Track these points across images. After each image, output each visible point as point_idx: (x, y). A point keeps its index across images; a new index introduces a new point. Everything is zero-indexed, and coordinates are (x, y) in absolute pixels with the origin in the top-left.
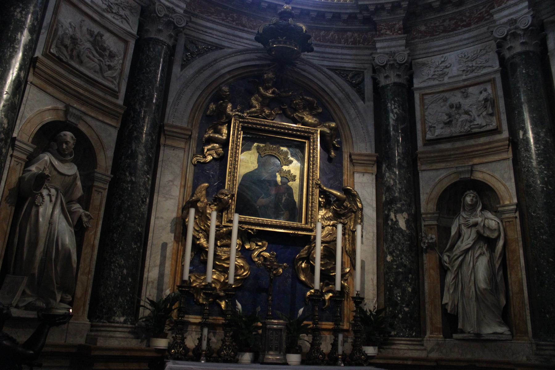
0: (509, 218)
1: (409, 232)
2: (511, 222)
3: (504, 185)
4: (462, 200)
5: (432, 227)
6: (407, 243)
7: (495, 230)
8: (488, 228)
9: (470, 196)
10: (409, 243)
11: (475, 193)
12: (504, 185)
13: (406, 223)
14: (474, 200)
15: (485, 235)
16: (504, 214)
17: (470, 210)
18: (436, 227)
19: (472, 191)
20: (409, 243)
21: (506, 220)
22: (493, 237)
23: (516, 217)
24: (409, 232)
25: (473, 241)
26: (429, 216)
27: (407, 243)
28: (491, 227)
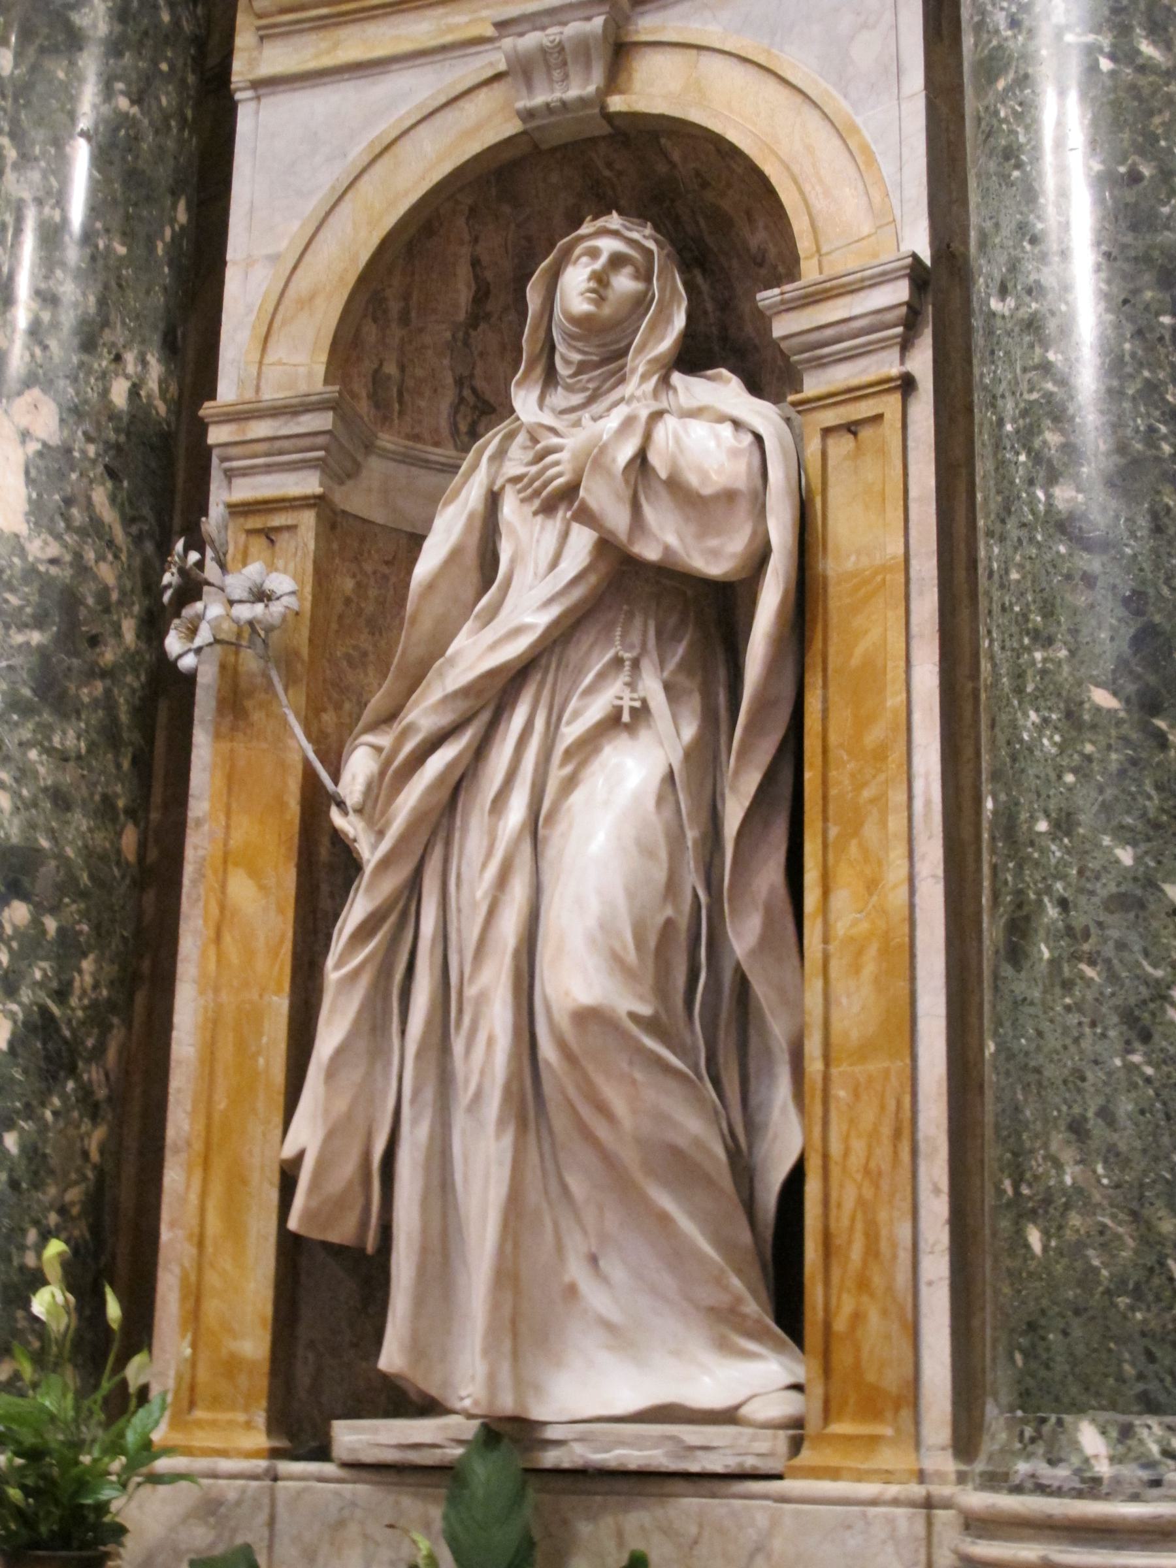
0: (854, 394)
1: (54, 550)
2: (866, 433)
3: (843, 132)
4: (533, 298)
5: (278, 520)
6: (18, 638)
7: (729, 496)
8: (675, 486)
9: (594, 253)
10: (36, 637)
11: (645, 235)
12: (843, 132)
13: (30, 481)
14: (624, 283)
15: (650, 553)
16: (821, 363)
17: (582, 368)
18: (308, 519)
19: (614, 221)
20: (36, 637)
21: (830, 417)
22: (716, 569)
23: (907, 384)
24: (54, 550)
25: (555, 611)
26: (261, 429)
27: (18, 638)
28: (693, 480)
